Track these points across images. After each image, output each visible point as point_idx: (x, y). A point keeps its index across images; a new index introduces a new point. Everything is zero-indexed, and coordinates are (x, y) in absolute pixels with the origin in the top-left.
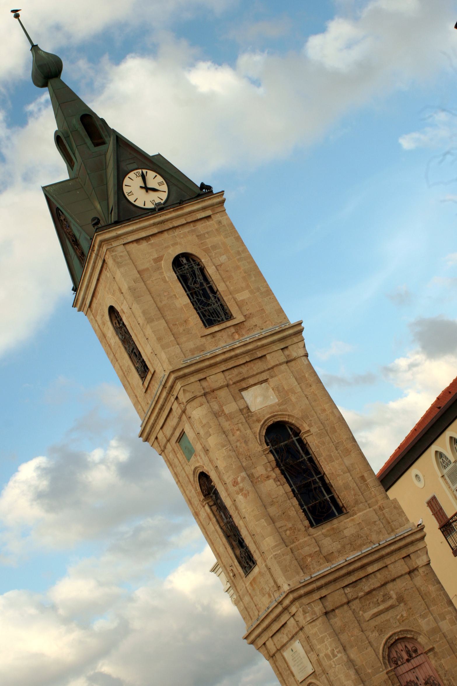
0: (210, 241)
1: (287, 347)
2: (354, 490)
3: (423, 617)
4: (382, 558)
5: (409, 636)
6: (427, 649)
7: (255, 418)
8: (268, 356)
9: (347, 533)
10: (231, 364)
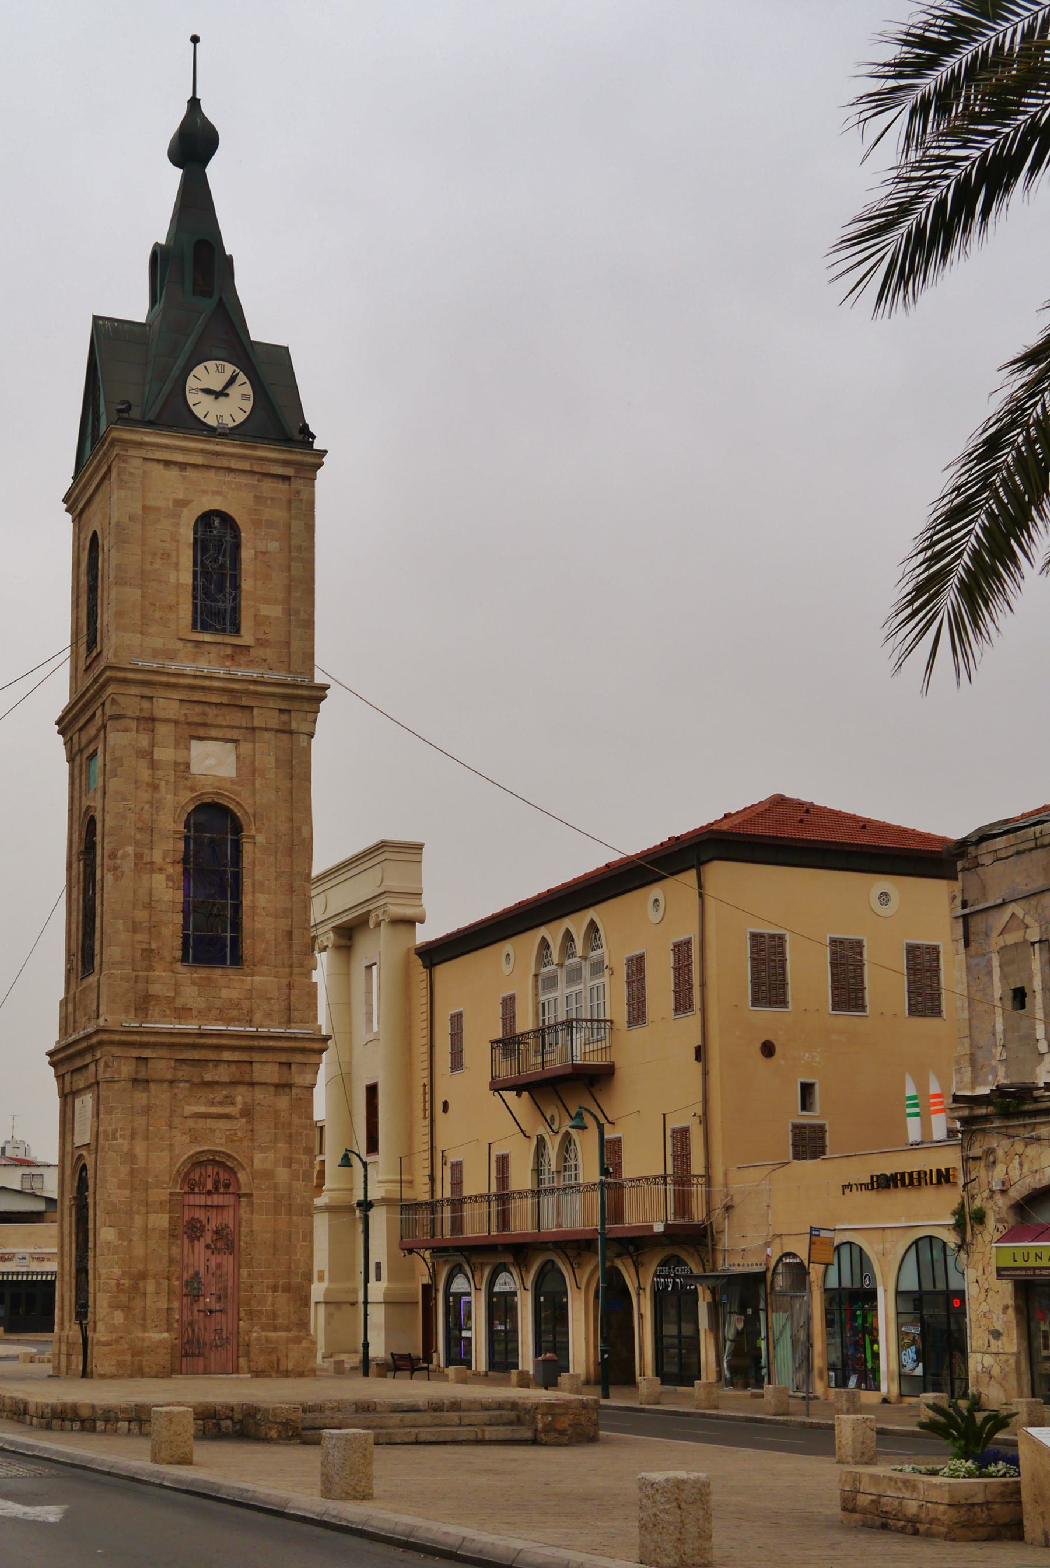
1: (289, 711)
2: (267, 943)
3: (263, 1149)
4: (250, 1049)
5: (228, 1163)
6: (243, 1191)
7: (189, 784)
8: (256, 711)
9: (225, 993)
10: (197, 696)
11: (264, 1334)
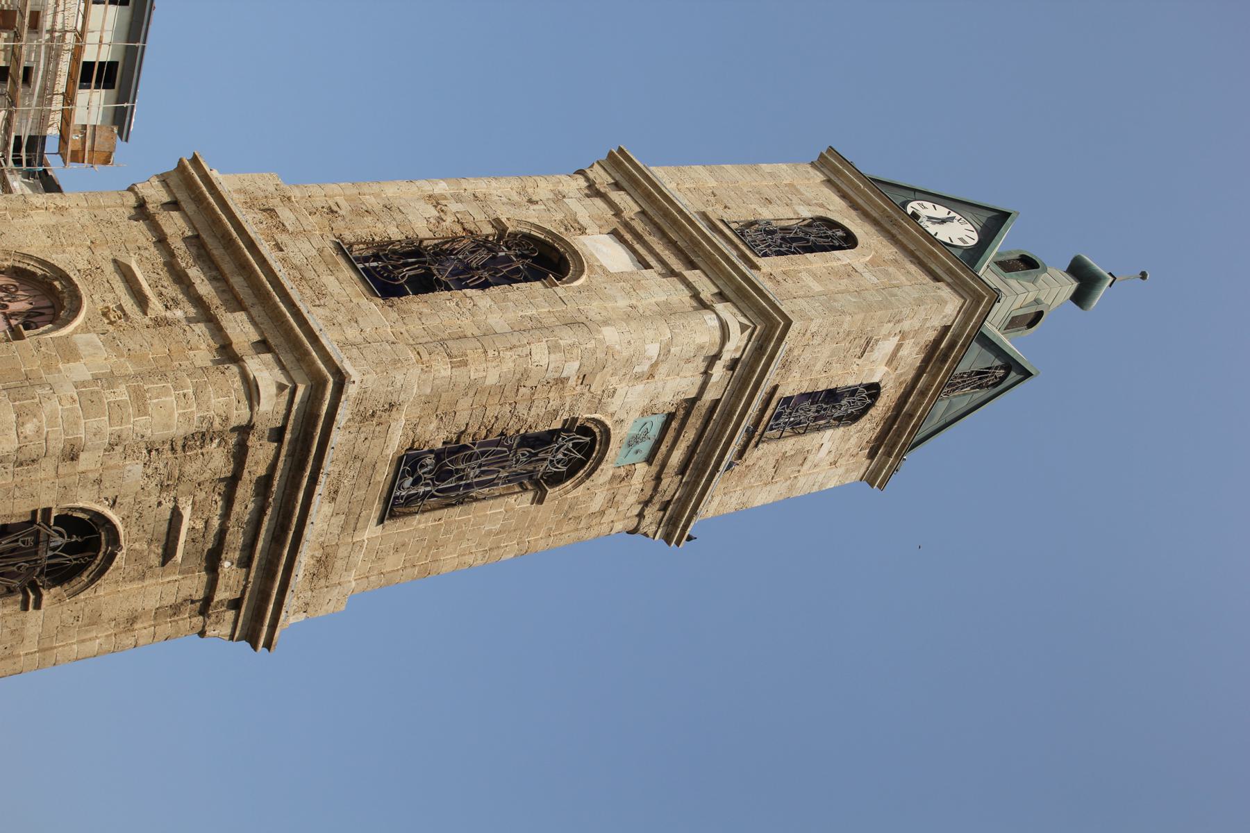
0: (891, 269)
3: (112, 343)
9: (330, 281)
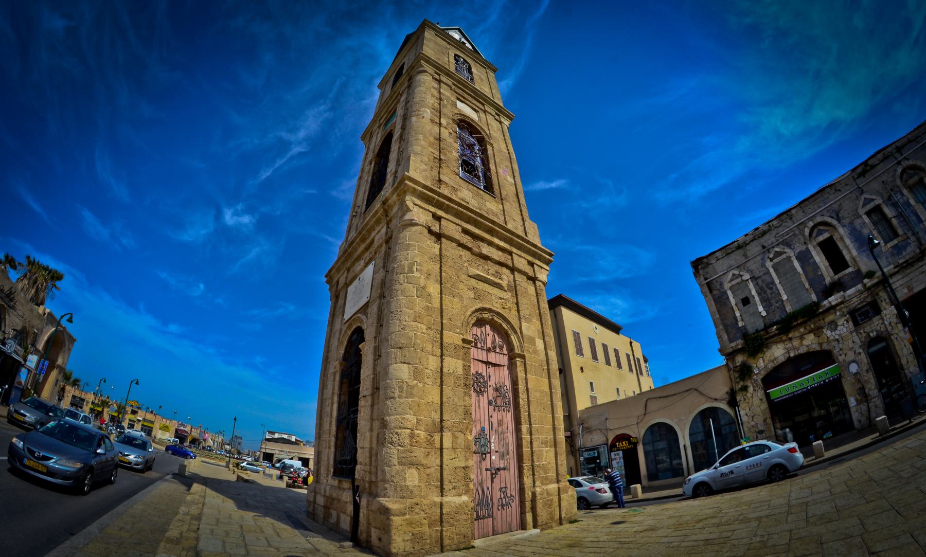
11: (544, 487)
